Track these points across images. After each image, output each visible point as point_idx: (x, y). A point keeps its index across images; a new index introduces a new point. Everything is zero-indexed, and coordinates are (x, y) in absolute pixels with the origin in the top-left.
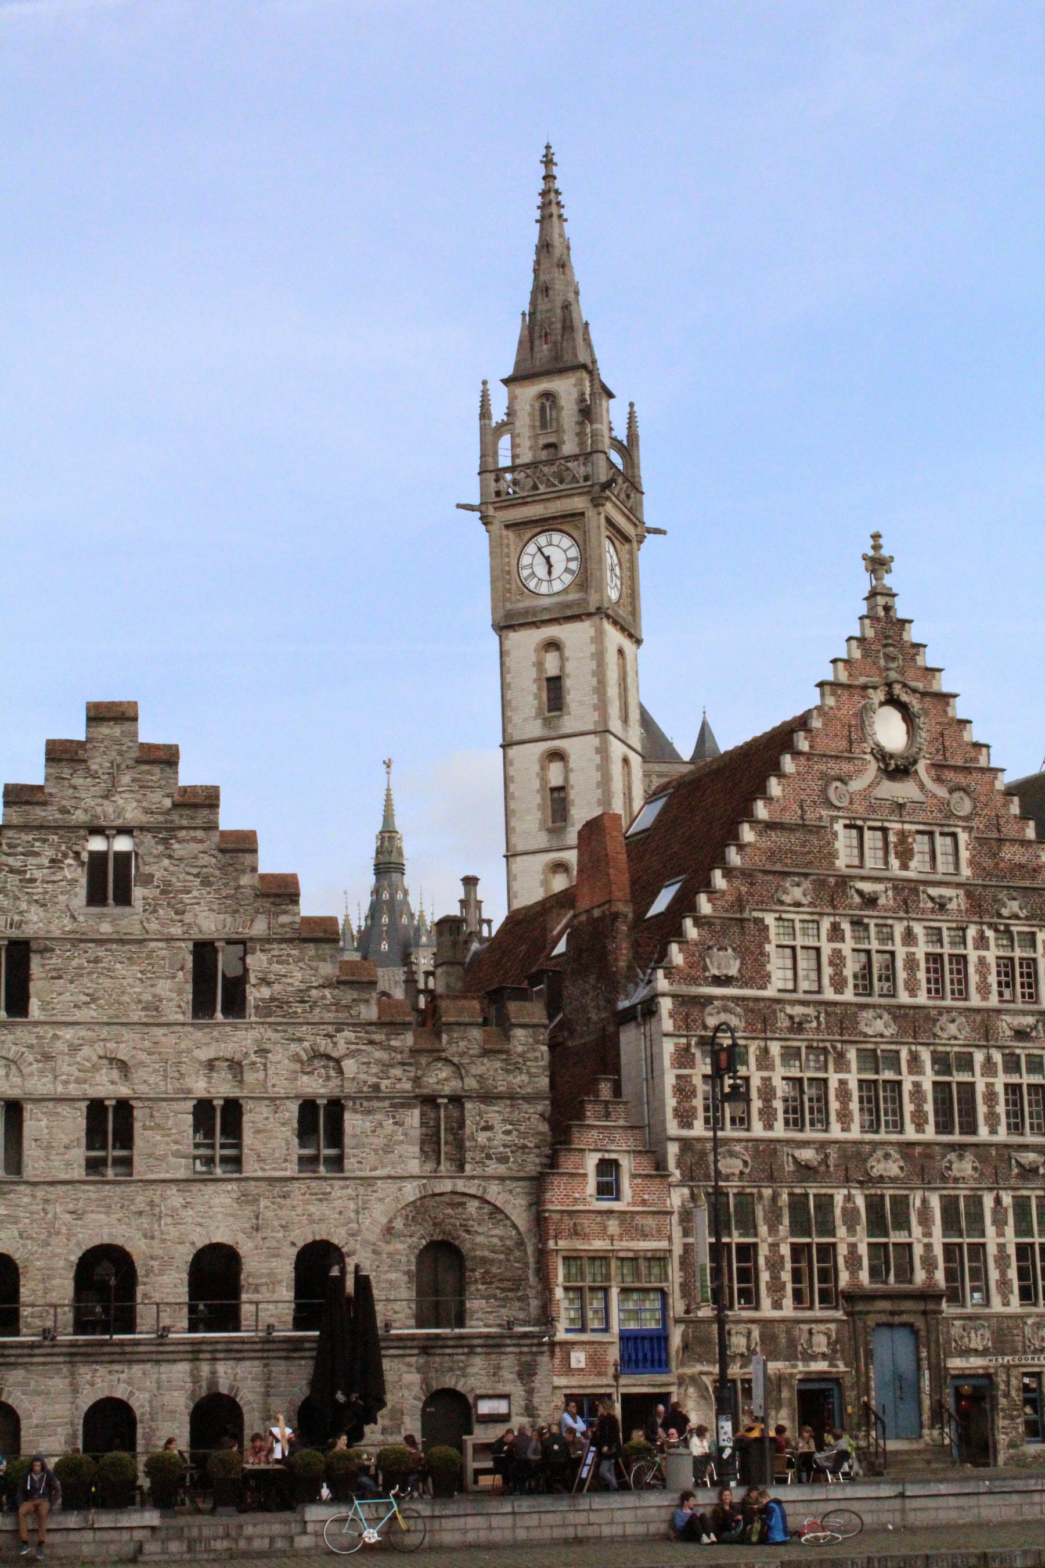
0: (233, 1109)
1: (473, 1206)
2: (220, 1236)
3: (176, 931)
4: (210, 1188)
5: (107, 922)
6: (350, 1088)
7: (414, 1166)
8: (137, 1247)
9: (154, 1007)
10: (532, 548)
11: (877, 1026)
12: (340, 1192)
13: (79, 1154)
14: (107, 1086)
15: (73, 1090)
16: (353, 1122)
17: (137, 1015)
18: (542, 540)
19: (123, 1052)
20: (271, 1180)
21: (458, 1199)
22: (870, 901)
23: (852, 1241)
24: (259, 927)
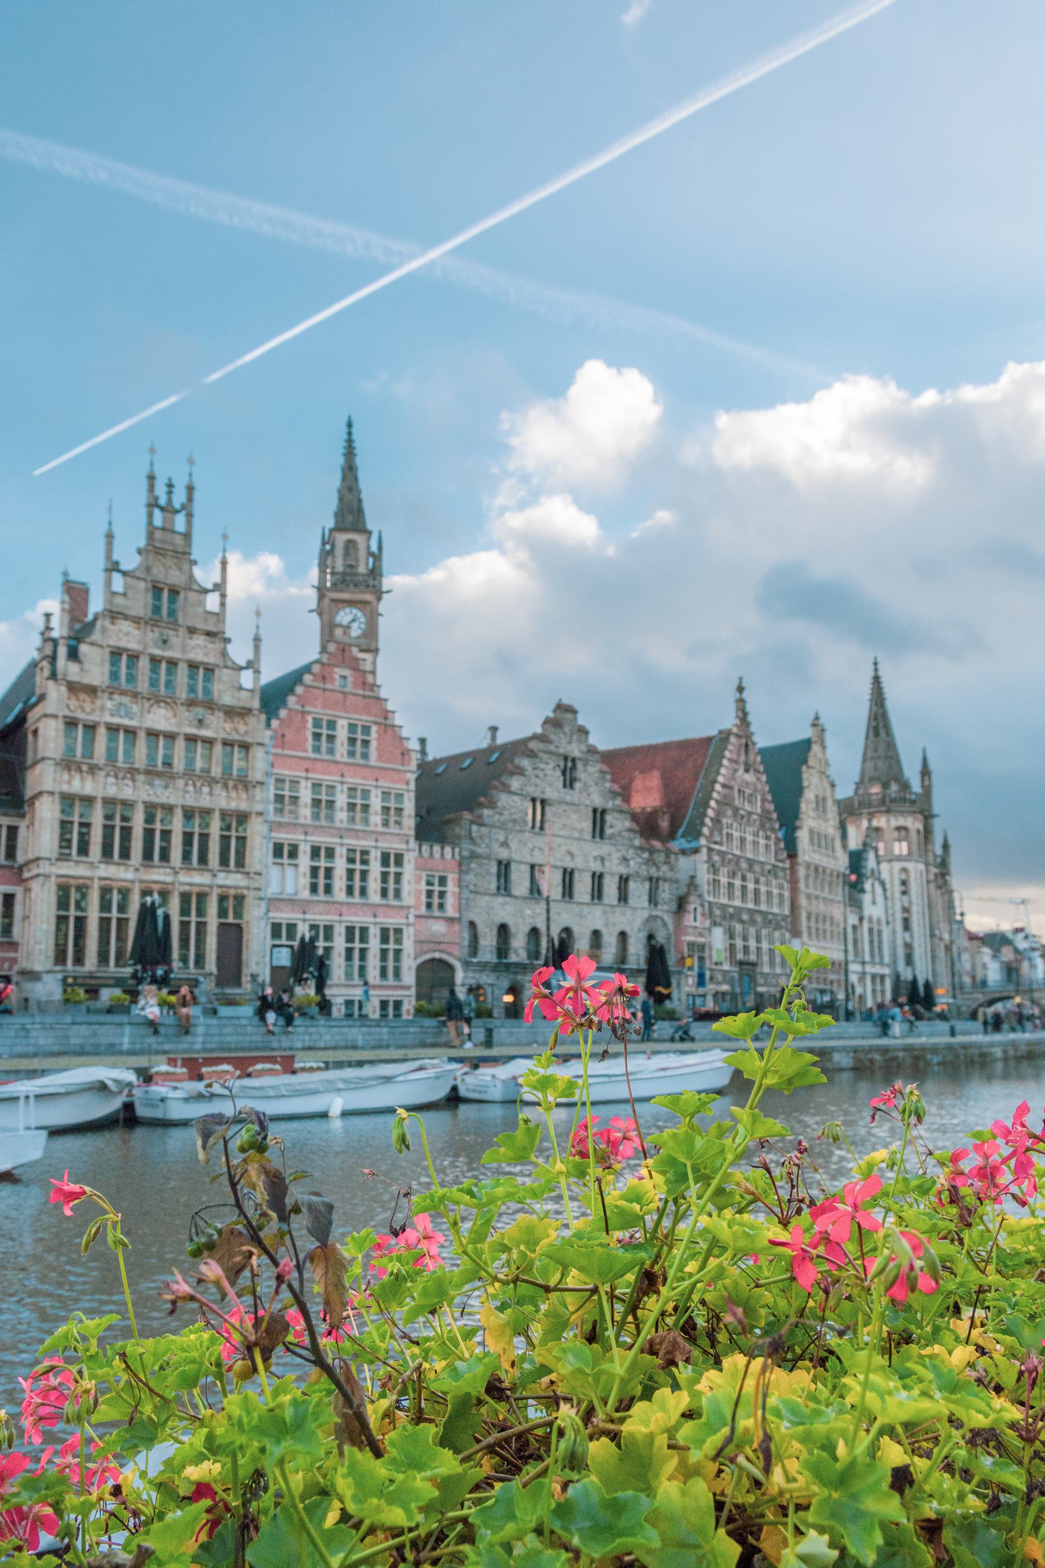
0: (601, 876)
1: (659, 921)
2: (598, 927)
3: (588, 802)
4: (595, 907)
5: (570, 796)
6: (631, 872)
7: (646, 904)
8: (576, 930)
9: (581, 831)
10: (342, 613)
11: (744, 865)
12: (629, 912)
13: (560, 889)
14: (570, 865)
15: (559, 863)
16: (632, 885)
17: (576, 835)
18: (347, 610)
19: (573, 850)
20: (612, 906)
21: (655, 918)
22: (742, 817)
23: (739, 943)
24: (610, 805)
